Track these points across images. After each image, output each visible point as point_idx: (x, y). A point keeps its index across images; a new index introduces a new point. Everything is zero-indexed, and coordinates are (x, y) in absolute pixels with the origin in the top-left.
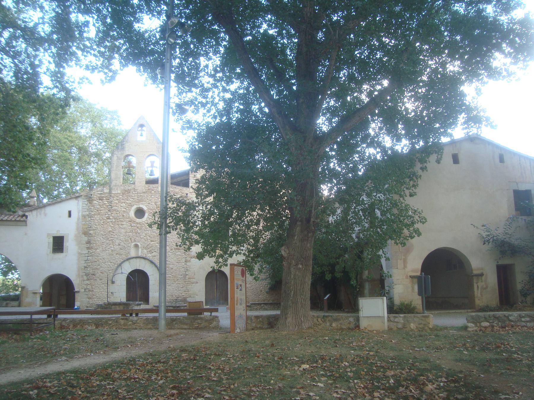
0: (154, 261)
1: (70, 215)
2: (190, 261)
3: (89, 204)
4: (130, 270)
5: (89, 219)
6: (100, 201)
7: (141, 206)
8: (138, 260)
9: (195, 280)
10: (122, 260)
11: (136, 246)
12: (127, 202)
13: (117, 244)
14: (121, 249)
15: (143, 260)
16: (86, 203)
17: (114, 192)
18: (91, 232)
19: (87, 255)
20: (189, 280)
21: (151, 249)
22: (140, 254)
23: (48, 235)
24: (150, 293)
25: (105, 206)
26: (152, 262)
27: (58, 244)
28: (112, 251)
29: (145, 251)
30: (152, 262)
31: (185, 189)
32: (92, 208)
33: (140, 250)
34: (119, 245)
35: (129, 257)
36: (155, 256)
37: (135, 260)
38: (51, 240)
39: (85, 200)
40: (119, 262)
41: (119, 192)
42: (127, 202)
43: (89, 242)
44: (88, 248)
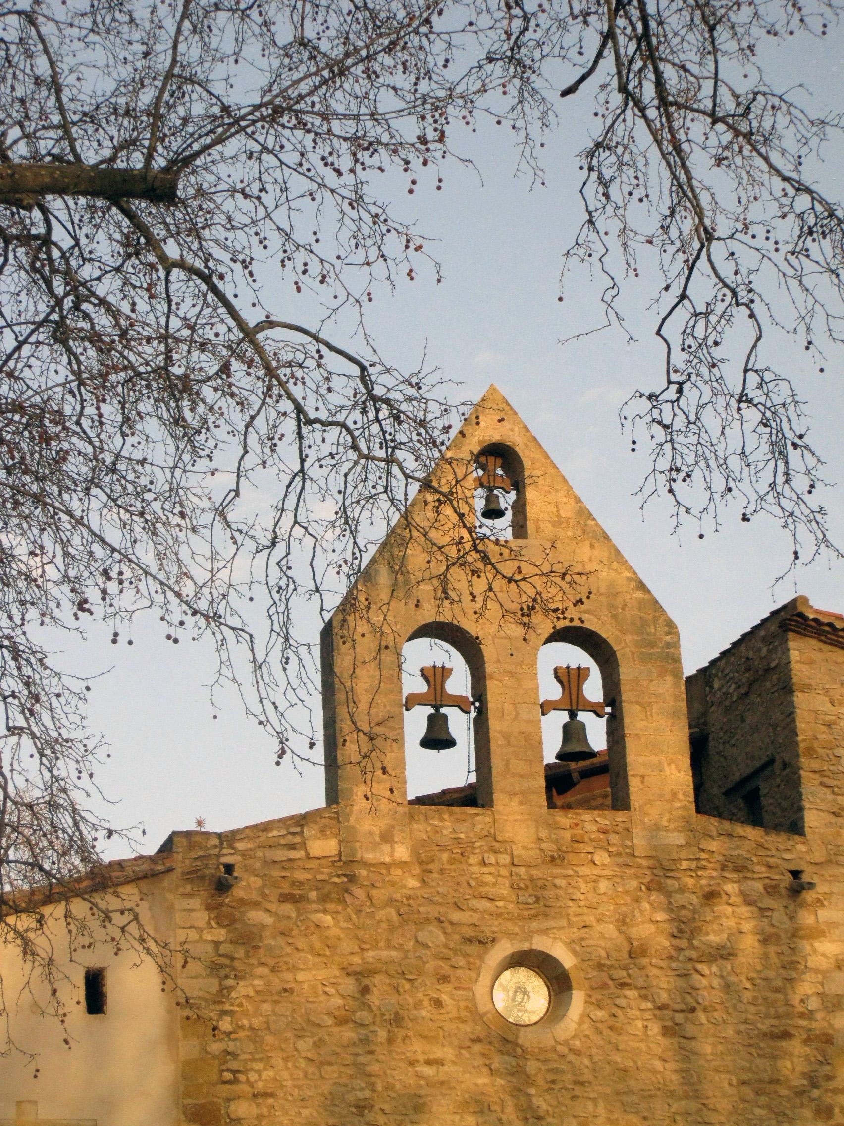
3: (223, 931)
6: (288, 909)
12: (456, 916)
16: (201, 917)
17: (369, 856)
25: (318, 945)
31: (776, 841)
32: (240, 953)
39: (195, 903)
41: (402, 852)
42: (456, 916)
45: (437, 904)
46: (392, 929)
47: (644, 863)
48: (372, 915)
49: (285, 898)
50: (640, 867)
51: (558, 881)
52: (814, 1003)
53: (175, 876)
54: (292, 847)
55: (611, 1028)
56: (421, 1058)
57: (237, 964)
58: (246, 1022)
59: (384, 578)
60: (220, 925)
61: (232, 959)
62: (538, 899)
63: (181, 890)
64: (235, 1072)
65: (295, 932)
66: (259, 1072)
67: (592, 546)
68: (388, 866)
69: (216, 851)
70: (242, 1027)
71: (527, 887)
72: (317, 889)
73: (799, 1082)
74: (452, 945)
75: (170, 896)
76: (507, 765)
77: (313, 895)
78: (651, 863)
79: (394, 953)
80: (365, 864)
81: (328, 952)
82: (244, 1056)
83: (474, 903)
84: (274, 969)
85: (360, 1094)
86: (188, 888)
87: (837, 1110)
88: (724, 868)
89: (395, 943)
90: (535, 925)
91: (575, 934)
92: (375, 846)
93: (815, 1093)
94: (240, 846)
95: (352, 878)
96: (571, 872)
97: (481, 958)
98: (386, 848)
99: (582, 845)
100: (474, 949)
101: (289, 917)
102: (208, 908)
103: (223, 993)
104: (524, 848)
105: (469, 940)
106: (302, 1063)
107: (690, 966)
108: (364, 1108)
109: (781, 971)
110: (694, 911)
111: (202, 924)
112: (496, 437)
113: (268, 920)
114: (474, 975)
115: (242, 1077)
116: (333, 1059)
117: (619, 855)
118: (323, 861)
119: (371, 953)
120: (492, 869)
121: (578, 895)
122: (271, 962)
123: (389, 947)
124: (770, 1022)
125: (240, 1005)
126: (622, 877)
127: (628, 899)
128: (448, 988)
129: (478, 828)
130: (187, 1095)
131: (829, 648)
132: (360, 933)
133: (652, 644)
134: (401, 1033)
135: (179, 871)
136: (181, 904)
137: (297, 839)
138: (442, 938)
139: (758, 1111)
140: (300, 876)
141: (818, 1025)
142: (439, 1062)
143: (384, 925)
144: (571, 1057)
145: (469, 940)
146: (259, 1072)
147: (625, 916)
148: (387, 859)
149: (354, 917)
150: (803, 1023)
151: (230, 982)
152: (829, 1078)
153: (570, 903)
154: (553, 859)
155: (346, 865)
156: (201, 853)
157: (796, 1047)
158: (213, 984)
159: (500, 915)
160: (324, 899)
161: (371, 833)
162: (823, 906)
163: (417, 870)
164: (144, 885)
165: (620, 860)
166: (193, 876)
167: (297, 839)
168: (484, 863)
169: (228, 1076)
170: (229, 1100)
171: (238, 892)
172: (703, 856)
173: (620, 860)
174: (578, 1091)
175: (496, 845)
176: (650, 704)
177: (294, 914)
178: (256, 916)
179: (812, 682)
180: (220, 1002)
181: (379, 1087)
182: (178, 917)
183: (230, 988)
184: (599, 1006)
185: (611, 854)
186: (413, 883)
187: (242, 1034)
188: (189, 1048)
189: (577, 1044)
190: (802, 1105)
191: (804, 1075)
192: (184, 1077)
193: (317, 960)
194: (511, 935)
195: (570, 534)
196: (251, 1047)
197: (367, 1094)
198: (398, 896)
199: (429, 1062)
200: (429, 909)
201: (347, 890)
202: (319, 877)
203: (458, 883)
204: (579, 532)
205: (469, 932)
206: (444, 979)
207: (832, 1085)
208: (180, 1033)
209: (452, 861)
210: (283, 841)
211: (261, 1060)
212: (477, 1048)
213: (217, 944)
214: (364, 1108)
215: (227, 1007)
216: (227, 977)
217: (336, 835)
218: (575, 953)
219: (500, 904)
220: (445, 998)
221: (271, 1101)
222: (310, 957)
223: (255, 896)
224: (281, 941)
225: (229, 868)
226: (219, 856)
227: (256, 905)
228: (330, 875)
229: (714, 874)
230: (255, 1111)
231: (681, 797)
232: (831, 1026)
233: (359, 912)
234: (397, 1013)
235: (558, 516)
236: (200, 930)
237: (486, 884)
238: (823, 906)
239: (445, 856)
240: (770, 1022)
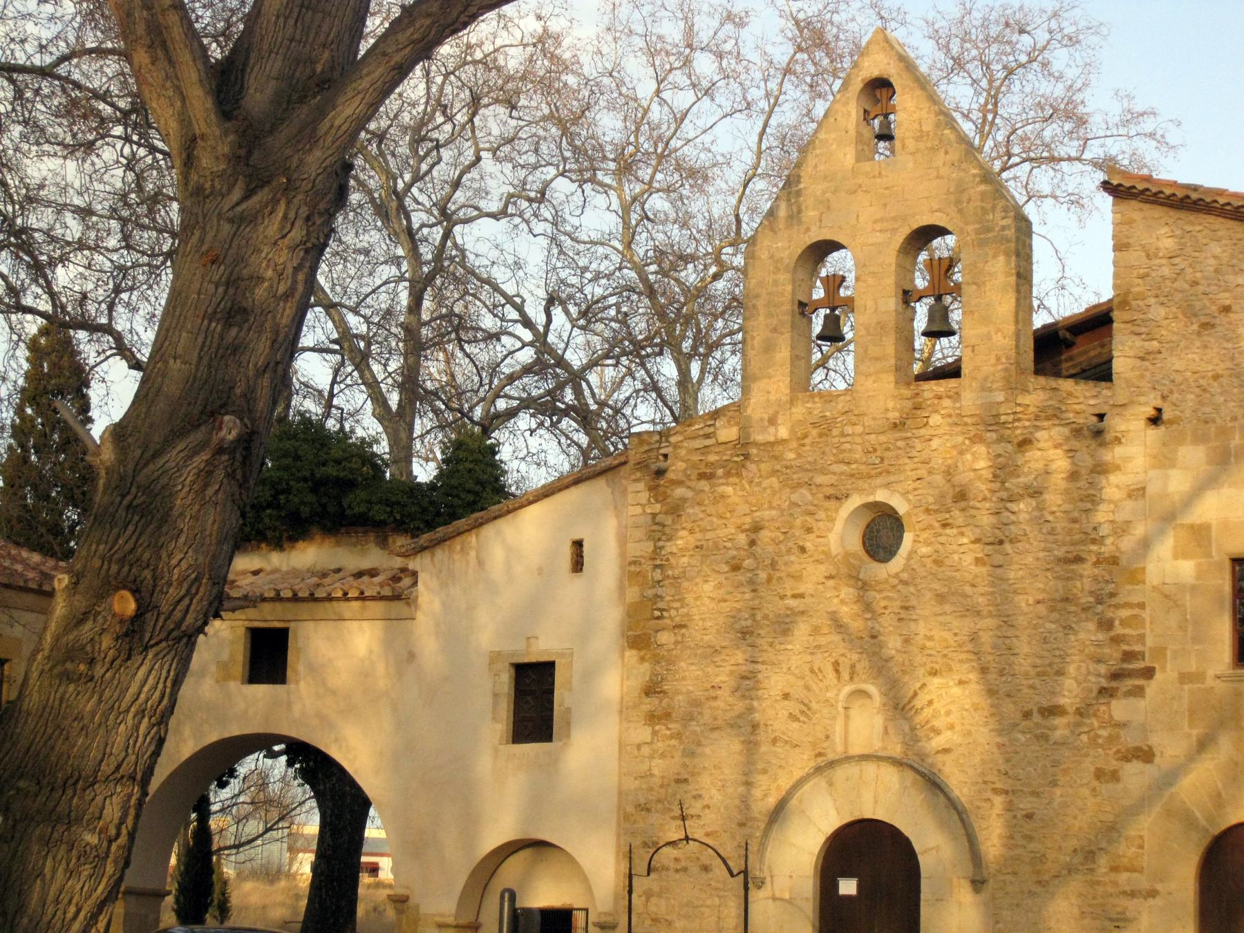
1: (578, 564)
2: (1115, 776)
3: (658, 506)
5: (658, 575)
6: (704, 485)
7: (881, 496)
9: (1143, 882)
12: (819, 479)
16: (644, 496)
17: (760, 438)
18: (665, 638)
19: (646, 750)
20: (1113, 876)
23: (495, 657)
27: (533, 701)
32: (668, 520)
38: (506, 680)
39: (641, 486)
41: (783, 432)
42: (819, 479)
43: (652, 689)
44: (653, 718)
45: (807, 470)
46: (774, 493)
47: (969, 420)
48: (759, 484)
49: (702, 476)
50: (966, 424)
51: (900, 444)
52: (1105, 530)
53: (627, 467)
54: (707, 436)
55: (935, 562)
56: (789, 593)
57: (667, 530)
58: (670, 573)
59: (782, 212)
60: (657, 501)
61: (664, 526)
62: (882, 459)
63: (633, 477)
64: (661, 610)
65: (706, 502)
66: (677, 609)
67: (946, 153)
68: (772, 444)
69: (657, 445)
70: (668, 577)
71: (875, 450)
72: (723, 467)
73: (1087, 599)
74: (816, 502)
75: (624, 482)
76: (866, 351)
77: (720, 472)
78: (974, 420)
79: (774, 512)
80: (756, 444)
81: (728, 515)
82: (668, 598)
83: (835, 468)
84: (692, 532)
85: (743, 623)
86: (638, 475)
87: (1117, 623)
88: (1037, 418)
89: (774, 504)
90: (878, 481)
91: (910, 485)
92: (764, 430)
93: (1100, 608)
94: (673, 439)
95: (747, 456)
96: (909, 435)
97: (837, 510)
98: (772, 430)
99: (919, 412)
100: (832, 504)
101: (703, 491)
102: (651, 489)
103: (657, 550)
104: (874, 419)
105: (828, 498)
106: (707, 601)
107: (1001, 505)
108: (746, 633)
109: (1079, 504)
110: (1010, 458)
111: (644, 501)
112: (876, 73)
113: (690, 494)
114: (830, 525)
115: (665, 614)
116: (728, 597)
117: (950, 416)
118: (729, 445)
119: (758, 514)
120: (849, 439)
121: (914, 453)
122: (689, 526)
123: (771, 508)
124: (1064, 549)
125: (668, 560)
126: (951, 435)
127: (955, 453)
128: (812, 536)
129: (840, 406)
130: (630, 629)
131: (1148, 205)
132: (750, 499)
133: (989, 230)
134: (778, 574)
135: (632, 462)
136: (633, 487)
137: (711, 430)
138: (809, 497)
139: (1048, 625)
140: (712, 458)
141: (1107, 549)
142: (802, 596)
143: (769, 491)
144: (900, 587)
145: (828, 498)
146: (677, 609)
147: (949, 467)
148: (772, 439)
149: (747, 486)
150: (1094, 548)
151: (661, 544)
152: (1112, 595)
153: (907, 461)
154: (895, 425)
155: (743, 446)
156: (647, 448)
157: (1087, 569)
158: (649, 546)
159: (852, 475)
160: (728, 474)
161: (762, 419)
162: (1120, 442)
163: (794, 444)
164: (609, 475)
165: (950, 420)
166: (642, 465)
167: (711, 430)
168: (843, 435)
169: (657, 613)
170: (657, 631)
171: (670, 475)
172: (1019, 409)
173: (950, 420)
174: (904, 614)
175: (854, 419)
176: (984, 283)
177: (707, 488)
178: (680, 492)
179: (1131, 241)
180: (654, 559)
181: (759, 617)
182: (630, 497)
183: (662, 548)
184: (928, 543)
185: (943, 416)
186: (791, 455)
187: (666, 582)
188: (633, 594)
189: (905, 576)
190: (1087, 620)
191: (1091, 593)
192: (629, 615)
193: (721, 522)
194: (860, 491)
195: (929, 145)
196: (673, 591)
197: (749, 623)
198: (778, 467)
199: (794, 596)
200: (800, 475)
201: (743, 466)
202: (725, 458)
203: (823, 453)
204: (936, 143)
205: (830, 491)
206: (809, 530)
207: (1114, 601)
208: (627, 583)
209: (821, 435)
210: (701, 433)
211: (679, 600)
212: (831, 583)
213: (654, 515)
214: (746, 633)
215: (658, 562)
216: (659, 539)
217: (738, 424)
218: (909, 501)
219: (854, 466)
220: (808, 545)
221: (684, 631)
222: (715, 520)
223: (680, 477)
224: (697, 509)
225: (666, 456)
226: (660, 448)
227: (679, 483)
228: (732, 455)
229: (1027, 424)
230: (673, 639)
231: (1004, 360)
232: (1118, 549)
233: (751, 482)
234: (773, 560)
235: (921, 131)
236: (643, 506)
237: (844, 451)
238: (1120, 442)
239: (815, 432)
240: (1064, 549)
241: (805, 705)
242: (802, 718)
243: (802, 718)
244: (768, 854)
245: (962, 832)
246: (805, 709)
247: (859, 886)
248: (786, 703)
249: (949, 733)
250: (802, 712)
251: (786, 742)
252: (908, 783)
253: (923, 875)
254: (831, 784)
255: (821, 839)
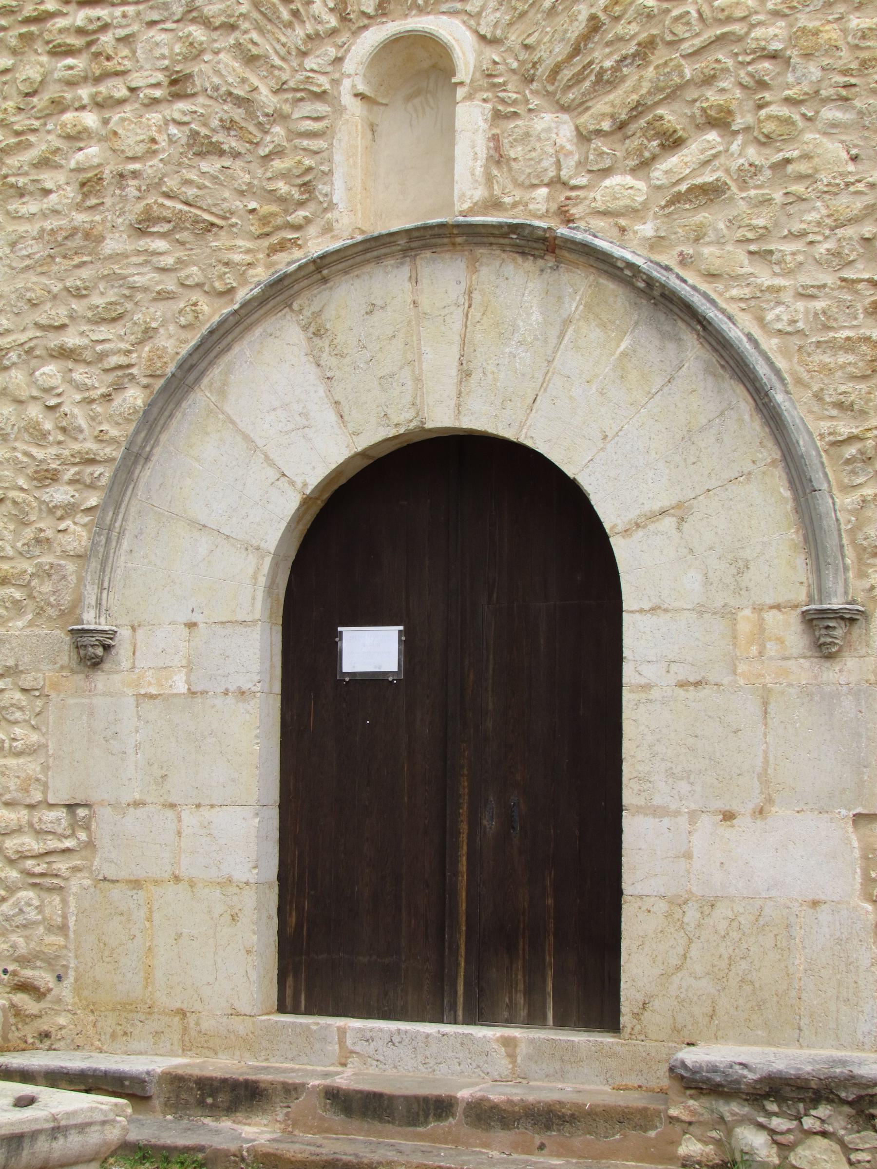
0: (689, 285)
4: (324, 452)
8: (444, 280)
10: (212, 312)
11: (418, 69)
13: (147, 76)
14: (210, 149)
15: (518, 291)
21: (637, 83)
22: (466, 192)
24: (642, 838)
26: (665, 303)
28: (90, 185)
29: (554, 129)
30: (665, 303)
33: (471, 118)
34: (178, 85)
35: (317, 245)
36: (711, 193)
37: (390, 283)
40: (174, 344)
241: (239, 101)
242: (231, 142)
243: (231, 142)
244: (122, 560)
245: (770, 452)
246: (238, 114)
247: (409, 648)
248: (182, 105)
249: (712, 136)
250: (229, 126)
251: (177, 223)
252: (572, 306)
253: (630, 599)
254: (317, 331)
255: (287, 504)
